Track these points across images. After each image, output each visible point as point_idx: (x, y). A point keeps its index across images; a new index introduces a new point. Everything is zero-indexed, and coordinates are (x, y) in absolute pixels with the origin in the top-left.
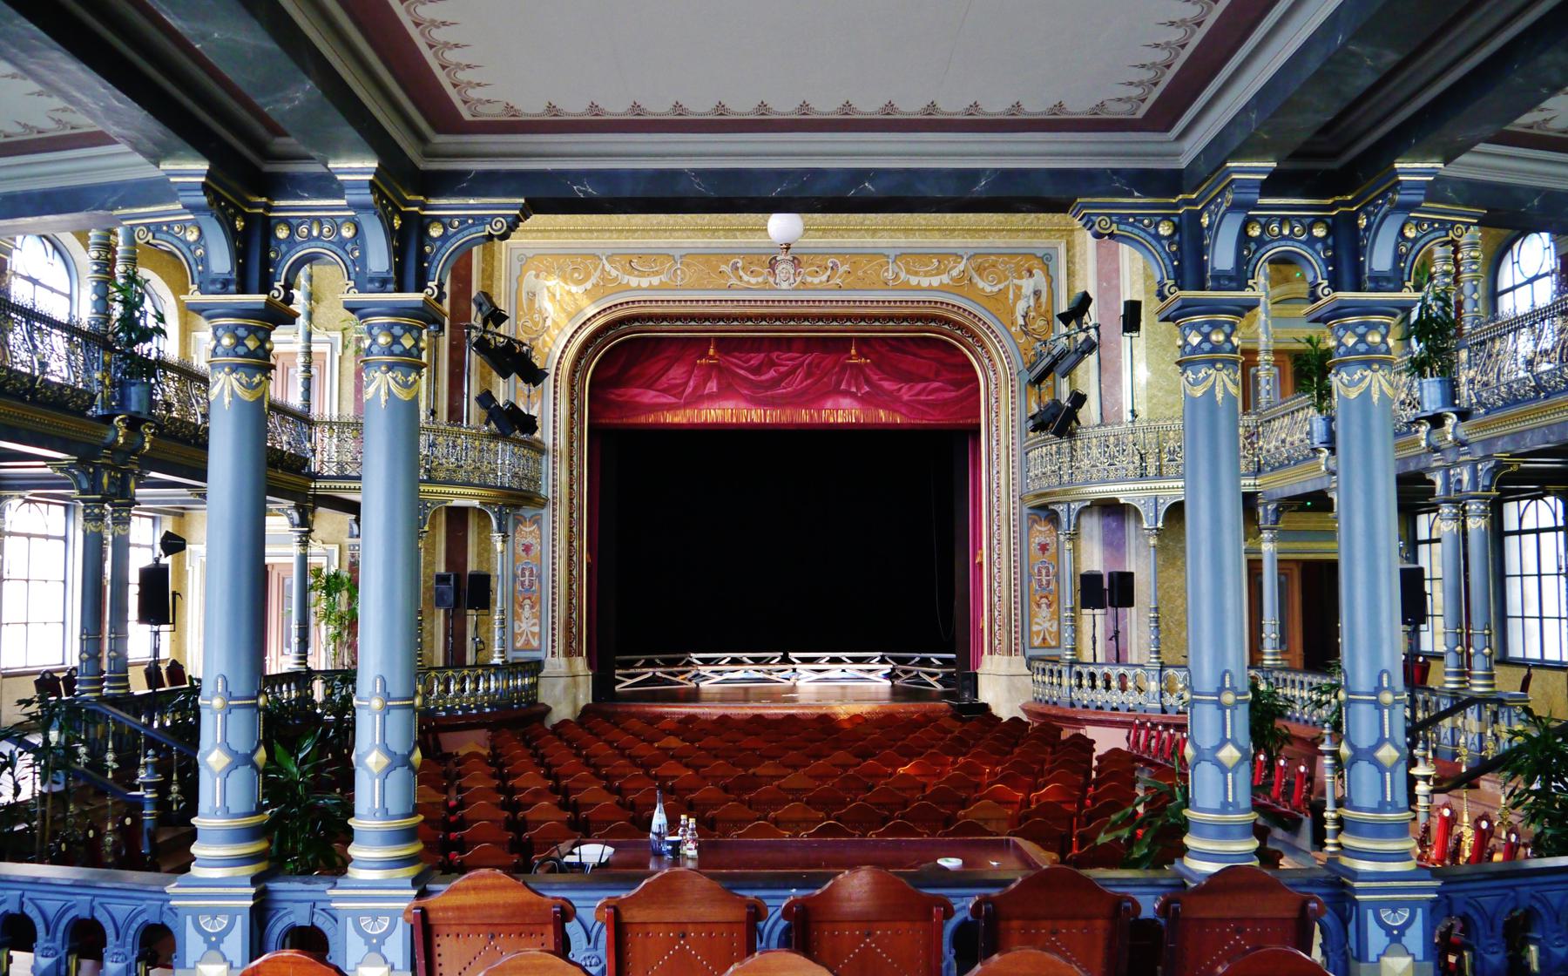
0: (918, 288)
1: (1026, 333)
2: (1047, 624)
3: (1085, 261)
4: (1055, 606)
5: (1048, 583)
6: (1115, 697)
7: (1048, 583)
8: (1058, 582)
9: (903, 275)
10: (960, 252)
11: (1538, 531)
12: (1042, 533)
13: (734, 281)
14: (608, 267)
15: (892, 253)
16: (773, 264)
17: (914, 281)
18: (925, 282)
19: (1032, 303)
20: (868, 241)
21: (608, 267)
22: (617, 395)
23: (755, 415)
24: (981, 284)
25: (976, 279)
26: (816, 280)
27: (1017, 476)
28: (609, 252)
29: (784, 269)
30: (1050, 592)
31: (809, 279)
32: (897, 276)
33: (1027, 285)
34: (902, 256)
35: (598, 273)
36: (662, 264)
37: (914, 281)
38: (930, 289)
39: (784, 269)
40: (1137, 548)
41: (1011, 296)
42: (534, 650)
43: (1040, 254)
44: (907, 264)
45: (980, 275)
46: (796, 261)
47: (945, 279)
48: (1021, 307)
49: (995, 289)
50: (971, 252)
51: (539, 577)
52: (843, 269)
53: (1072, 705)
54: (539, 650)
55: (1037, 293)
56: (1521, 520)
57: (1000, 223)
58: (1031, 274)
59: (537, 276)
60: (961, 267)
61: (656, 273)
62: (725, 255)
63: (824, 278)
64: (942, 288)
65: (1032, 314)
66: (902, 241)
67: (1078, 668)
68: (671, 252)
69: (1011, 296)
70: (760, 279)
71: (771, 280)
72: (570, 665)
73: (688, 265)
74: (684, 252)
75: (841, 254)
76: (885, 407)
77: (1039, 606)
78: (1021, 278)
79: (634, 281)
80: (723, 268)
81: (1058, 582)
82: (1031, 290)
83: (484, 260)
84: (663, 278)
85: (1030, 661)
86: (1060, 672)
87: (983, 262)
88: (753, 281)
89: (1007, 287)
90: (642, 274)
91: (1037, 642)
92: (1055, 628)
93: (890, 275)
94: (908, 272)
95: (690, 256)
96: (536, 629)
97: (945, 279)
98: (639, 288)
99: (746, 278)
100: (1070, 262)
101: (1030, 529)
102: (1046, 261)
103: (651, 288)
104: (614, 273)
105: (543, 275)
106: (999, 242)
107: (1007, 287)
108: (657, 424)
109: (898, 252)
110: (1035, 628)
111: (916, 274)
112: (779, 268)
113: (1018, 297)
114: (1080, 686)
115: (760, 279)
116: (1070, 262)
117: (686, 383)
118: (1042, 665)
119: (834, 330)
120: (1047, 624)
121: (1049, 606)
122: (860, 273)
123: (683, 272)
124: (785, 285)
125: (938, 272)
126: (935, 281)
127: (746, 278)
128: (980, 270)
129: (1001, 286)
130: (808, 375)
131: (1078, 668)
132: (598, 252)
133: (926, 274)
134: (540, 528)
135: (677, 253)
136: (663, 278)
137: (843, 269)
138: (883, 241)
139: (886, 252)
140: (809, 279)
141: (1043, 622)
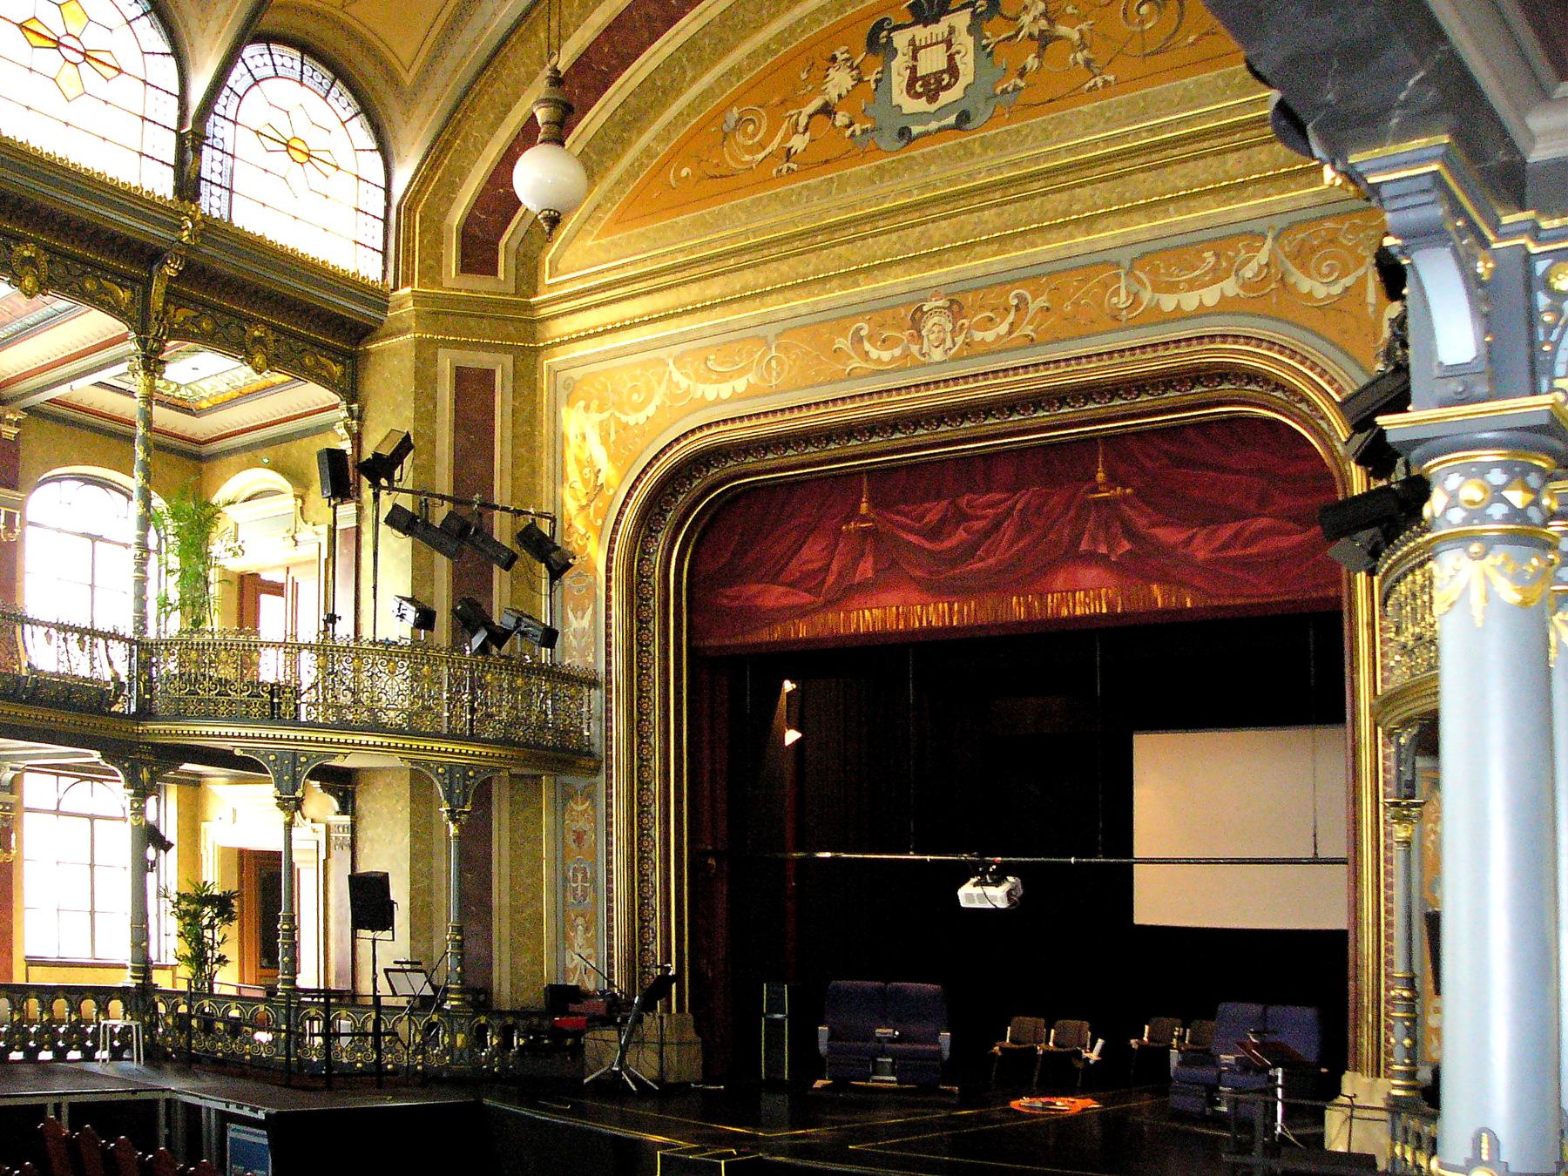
0: (1179, 316)
9: (1146, 296)
10: (1258, 227)
13: (856, 363)
14: (677, 376)
15: (1125, 257)
17: (1168, 303)
18: (1190, 301)
20: (1081, 241)
21: (677, 376)
22: (729, 597)
23: (933, 614)
24: (1305, 285)
26: (990, 336)
31: (978, 336)
36: (751, 354)
37: (1168, 303)
38: (1202, 312)
44: (1154, 272)
45: (1303, 268)
46: (955, 308)
47: (1230, 287)
49: (1337, 289)
50: (1280, 223)
52: (1033, 306)
60: (1263, 257)
61: (742, 372)
63: (1003, 328)
64: (1225, 307)
66: (1141, 227)
70: (897, 352)
71: (915, 349)
75: (1031, 277)
76: (1164, 579)
80: (843, 343)
84: (752, 377)
88: (886, 356)
90: (723, 378)
93: (1122, 300)
94: (1156, 289)
97: (1230, 287)
99: (874, 353)
104: (684, 383)
108: (787, 642)
109: (1135, 252)
111: (1172, 288)
115: (897, 352)
117: (829, 565)
123: (780, 363)
124: (937, 355)
125: (1216, 276)
126: (1210, 296)
127: (874, 353)
128: (1301, 257)
129: (1348, 281)
130: (1020, 533)
133: (1192, 286)
136: (752, 377)
138: (1106, 236)
139: (1113, 256)
140: (978, 336)
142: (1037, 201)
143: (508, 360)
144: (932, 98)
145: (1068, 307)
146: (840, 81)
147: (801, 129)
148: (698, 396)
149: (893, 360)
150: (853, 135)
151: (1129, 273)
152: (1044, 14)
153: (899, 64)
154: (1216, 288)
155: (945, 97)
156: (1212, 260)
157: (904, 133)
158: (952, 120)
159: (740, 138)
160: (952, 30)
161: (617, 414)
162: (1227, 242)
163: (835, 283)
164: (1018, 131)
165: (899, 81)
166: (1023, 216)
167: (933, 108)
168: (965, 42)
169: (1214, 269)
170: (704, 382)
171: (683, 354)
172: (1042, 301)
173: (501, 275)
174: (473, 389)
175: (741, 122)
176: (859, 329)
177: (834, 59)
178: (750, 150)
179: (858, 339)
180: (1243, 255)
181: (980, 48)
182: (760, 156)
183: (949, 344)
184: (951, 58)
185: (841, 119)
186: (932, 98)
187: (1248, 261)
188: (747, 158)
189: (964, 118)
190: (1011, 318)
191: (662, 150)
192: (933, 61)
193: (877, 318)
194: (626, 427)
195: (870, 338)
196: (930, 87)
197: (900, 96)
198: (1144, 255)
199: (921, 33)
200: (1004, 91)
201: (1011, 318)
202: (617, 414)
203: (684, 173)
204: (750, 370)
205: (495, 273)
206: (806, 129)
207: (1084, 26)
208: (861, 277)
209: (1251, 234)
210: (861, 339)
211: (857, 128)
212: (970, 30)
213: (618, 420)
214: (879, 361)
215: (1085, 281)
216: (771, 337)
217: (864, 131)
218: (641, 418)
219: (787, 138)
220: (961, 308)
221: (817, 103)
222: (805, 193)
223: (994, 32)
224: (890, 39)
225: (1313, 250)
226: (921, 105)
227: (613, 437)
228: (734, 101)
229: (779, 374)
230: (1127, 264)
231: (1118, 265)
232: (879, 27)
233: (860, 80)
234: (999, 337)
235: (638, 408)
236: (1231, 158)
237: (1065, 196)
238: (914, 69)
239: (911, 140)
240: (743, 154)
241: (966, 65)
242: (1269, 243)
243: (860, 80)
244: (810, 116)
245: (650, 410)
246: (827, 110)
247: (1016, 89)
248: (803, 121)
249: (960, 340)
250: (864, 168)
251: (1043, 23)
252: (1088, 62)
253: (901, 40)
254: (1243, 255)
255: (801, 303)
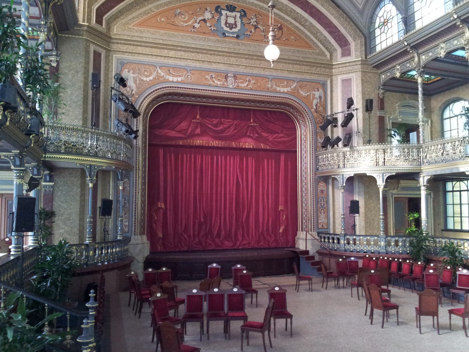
0: (279, 92)
1: (317, 112)
2: (324, 220)
3: (337, 87)
4: (326, 213)
5: (324, 204)
6: (358, 248)
7: (324, 205)
8: (327, 204)
9: (274, 86)
10: (294, 80)
11: (460, 191)
12: (322, 186)
14: (160, 71)
15: (271, 78)
16: (226, 77)
18: (282, 90)
19: (318, 101)
21: (160, 71)
24: (301, 92)
25: (300, 90)
26: (243, 85)
27: (314, 165)
28: (161, 65)
29: (230, 80)
30: (325, 208)
31: (240, 85)
32: (272, 87)
33: (317, 94)
34: (274, 79)
35: (156, 72)
36: (182, 72)
37: (278, 89)
38: (284, 93)
39: (230, 80)
40: (359, 192)
41: (311, 98)
42: (126, 233)
43: (321, 83)
44: (275, 82)
46: (235, 77)
47: (289, 89)
48: (315, 102)
49: (306, 95)
51: (129, 201)
52: (253, 82)
53: (345, 251)
54: (128, 232)
55: (320, 97)
56: (453, 188)
57: (308, 70)
58: (318, 90)
59: (129, 72)
60: (295, 85)
61: (180, 76)
62: (208, 71)
63: (246, 85)
64: (287, 93)
65: (318, 105)
67: (348, 237)
68: (186, 68)
69: (311, 98)
70: (221, 83)
71: (226, 83)
72: (142, 238)
73: (193, 74)
74: (191, 68)
75: (251, 75)
77: (321, 213)
78: (315, 91)
79: (171, 79)
80: (207, 77)
81: (327, 204)
82: (318, 96)
83: (106, 62)
84: (183, 78)
85: (319, 233)
86: (338, 240)
87: (302, 83)
88: (219, 83)
89: (310, 94)
90: (174, 76)
91: (320, 227)
92: (326, 221)
93: (270, 86)
94: (276, 85)
95: (193, 70)
96: (127, 224)
97: (289, 89)
98: (173, 82)
99: (216, 82)
100: (332, 87)
101: (318, 184)
102: (324, 85)
103: (178, 82)
104: (162, 74)
105: (131, 72)
106: (308, 77)
107: (310, 94)
110: (320, 221)
111: (279, 86)
112: (229, 79)
113: (314, 98)
114: (349, 243)
115: (221, 83)
116: (332, 87)
118: (324, 235)
119: (247, 106)
120: (324, 220)
121: (324, 213)
122: (259, 84)
123: (191, 77)
124: (231, 86)
125: (287, 86)
126: (286, 90)
128: (301, 87)
129: (308, 94)
131: (348, 237)
132: (155, 64)
133: (283, 87)
134: (129, 180)
135: (189, 69)
136: (183, 78)
137: (253, 82)
139: (268, 77)
140: (240, 85)
141: (322, 219)
142: (254, 61)
143: (105, 51)
144: (231, 29)
145: (259, 84)
146: (208, 15)
147: (197, 22)
148: (167, 78)
149: (220, 84)
150: (211, 29)
151: (271, 81)
152: (256, 22)
153: (223, 18)
154: (287, 89)
155: (234, 30)
156: (286, 83)
157: (224, 34)
158: (235, 36)
159: (180, 18)
160: (236, 16)
161: (140, 76)
162: (289, 80)
163: (206, 63)
164: (250, 44)
165: (223, 22)
166: (250, 62)
167: (231, 31)
168: (239, 20)
169: (286, 85)
170: (169, 75)
171: (162, 66)
172: (254, 81)
173: (104, 26)
174: (97, 56)
175: (180, 14)
176: (212, 75)
177: (207, 9)
178: (183, 22)
179: (212, 77)
180: (291, 84)
181: (242, 23)
182: (186, 24)
183: (233, 84)
184: (235, 22)
185: (208, 24)
186: (231, 29)
187: (291, 85)
188: (182, 24)
189: (238, 37)
190: (247, 83)
191: (156, 11)
192: (231, 21)
193: (217, 74)
194: (142, 80)
195: (215, 78)
196: (231, 26)
197: (223, 25)
198: (274, 78)
199: (229, 13)
200: (247, 34)
201: (247, 83)
202: (140, 76)
203: (163, 19)
204: (182, 76)
205: (102, 25)
206: (199, 23)
207: (264, 28)
208: (213, 64)
209: (293, 80)
210: (213, 78)
211: (212, 28)
212: (240, 17)
213: (140, 78)
214: (217, 84)
215: (262, 80)
216: (189, 70)
217: (214, 30)
218: (148, 79)
219: (193, 23)
220: (237, 78)
221: (202, 18)
222: (198, 38)
223: (245, 20)
224: (221, 12)
225: (303, 87)
226: (228, 29)
227: (138, 82)
228: (178, 7)
229: (191, 80)
230: (271, 79)
231: (269, 79)
232: (218, 7)
233: (213, 17)
234: (244, 86)
235: (147, 76)
236: (290, 65)
237: (259, 61)
238: (227, 21)
239: (226, 36)
240: (180, 21)
241: (239, 24)
242: (296, 83)
243: (213, 17)
244: (200, 20)
245: (151, 78)
246: (204, 20)
247: (250, 35)
248: (198, 21)
249: (236, 84)
250: (215, 38)
251: (255, 23)
252: (264, 36)
253: (224, 12)
254: (291, 84)
255: (198, 65)
